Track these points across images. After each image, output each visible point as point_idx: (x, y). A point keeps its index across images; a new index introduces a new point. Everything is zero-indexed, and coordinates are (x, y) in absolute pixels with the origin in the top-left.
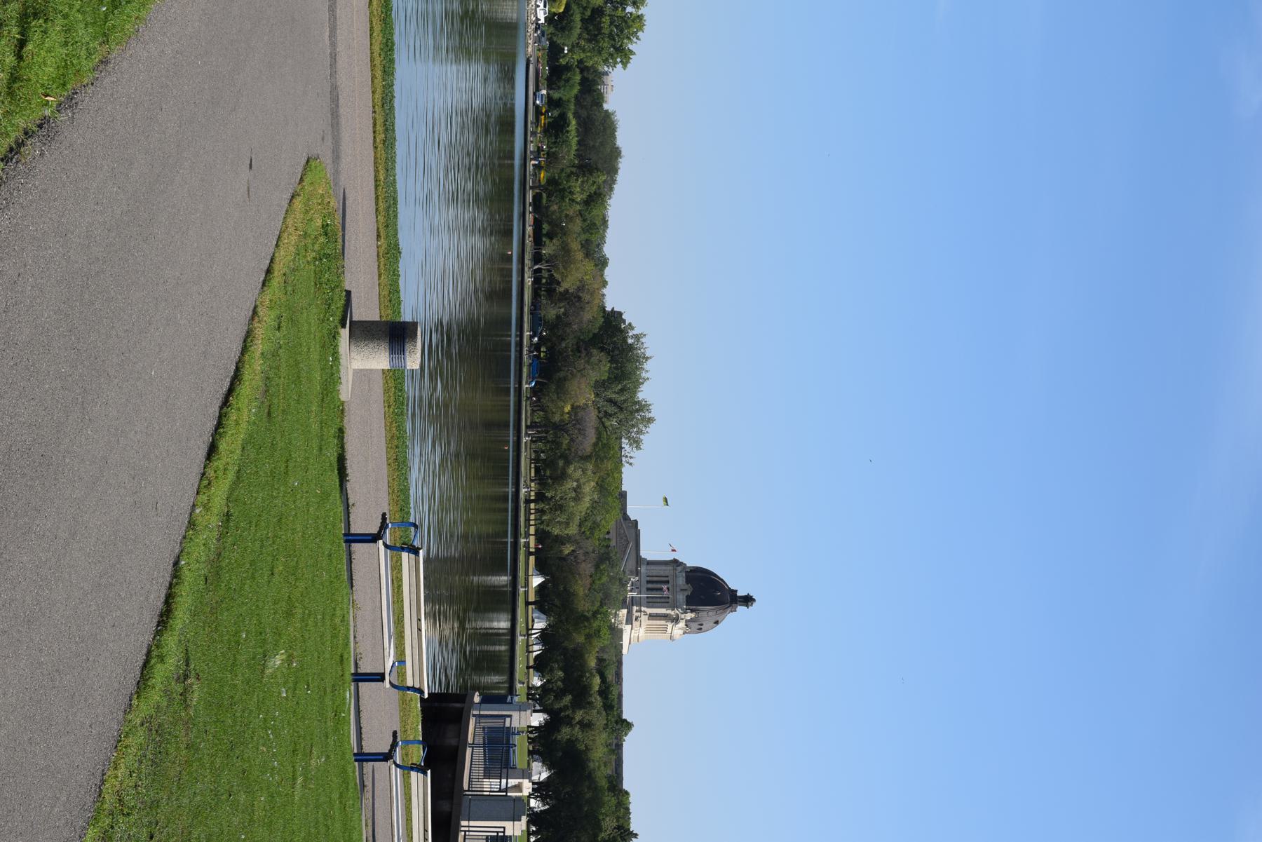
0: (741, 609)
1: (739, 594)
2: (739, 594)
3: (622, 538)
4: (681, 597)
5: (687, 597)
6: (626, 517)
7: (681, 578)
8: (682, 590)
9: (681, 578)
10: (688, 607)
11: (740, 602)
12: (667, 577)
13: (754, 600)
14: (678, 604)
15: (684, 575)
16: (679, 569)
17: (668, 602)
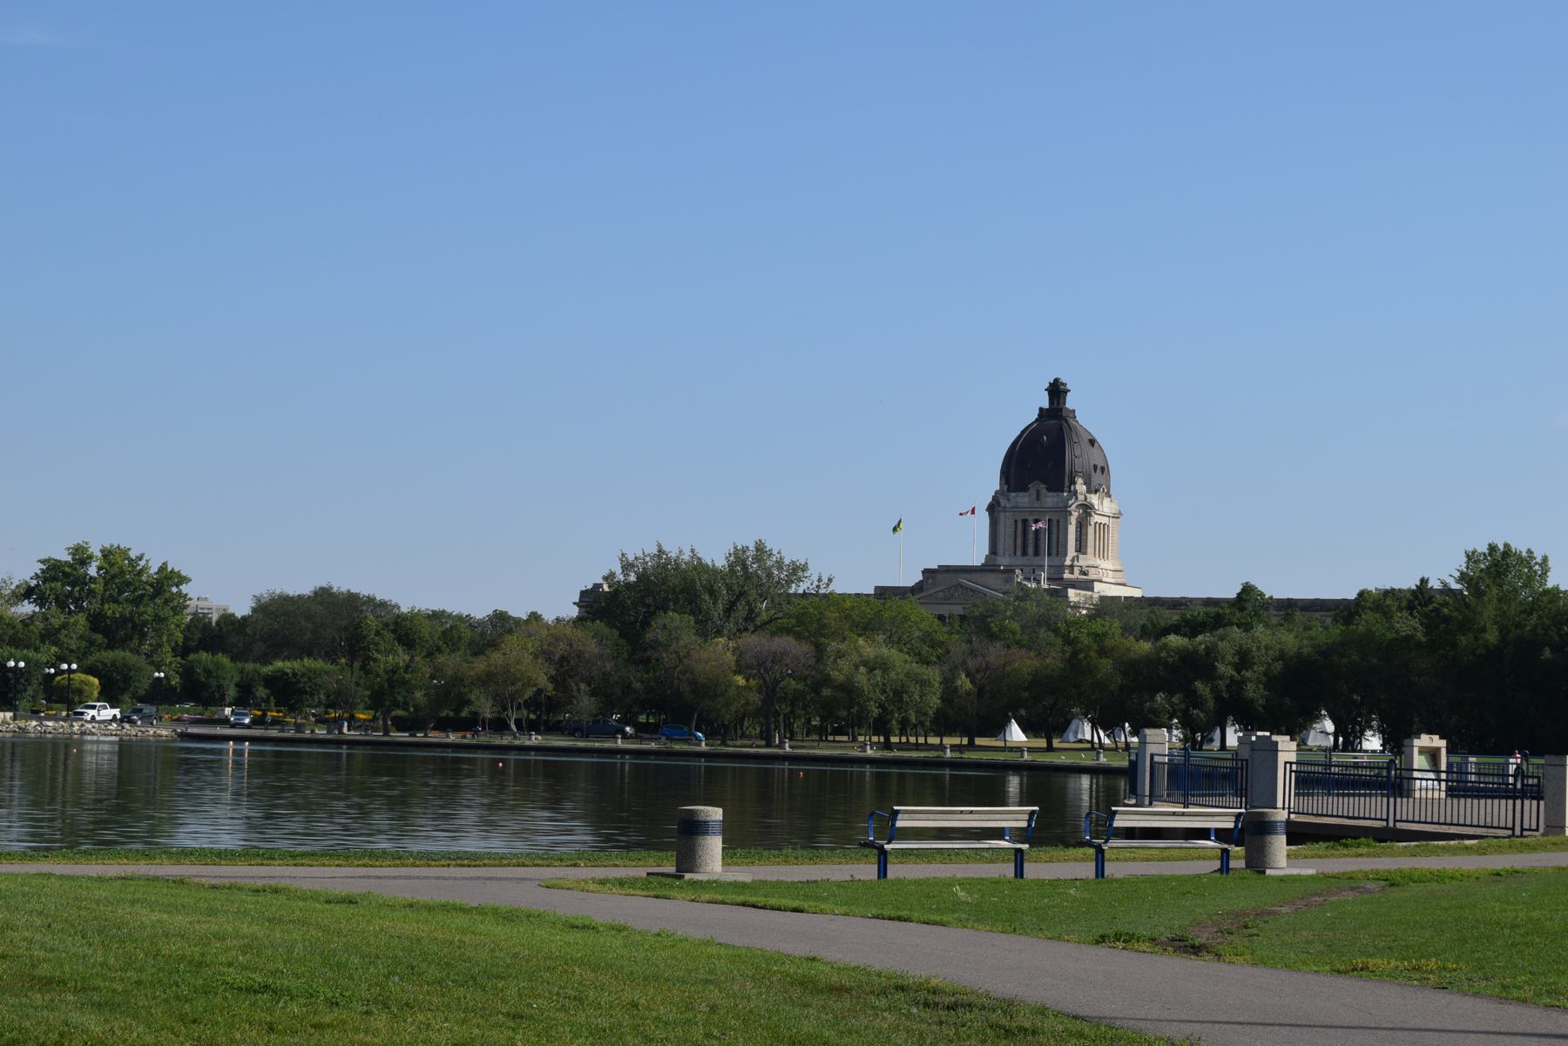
0: (1070, 402)
1: (1046, 405)
2: (1046, 405)
5: (1049, 490)
6: (917, 589)
7: (1019, 500)
8: (1038, 498)
9: (1019, 500)
10: (1066, 489)
11: (1058, 403)
12: (1016, 521)
13: (1056, 380)
14: (1061, 505)
15: (1013, 494)
16: (1003, 502)
17: (1058, 521)
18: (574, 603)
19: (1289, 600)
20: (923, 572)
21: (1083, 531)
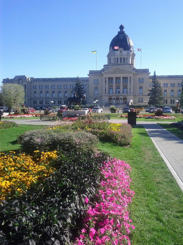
0: (124, 30)
1: (120, 31)
2: (120, 31)
5: (124, 50)
6: (103, 70)
8: (121, 52)
11: (123, 30)
13: (122, 25)
18: (2, 82)
20: (104, 66)
21: (132, 61)
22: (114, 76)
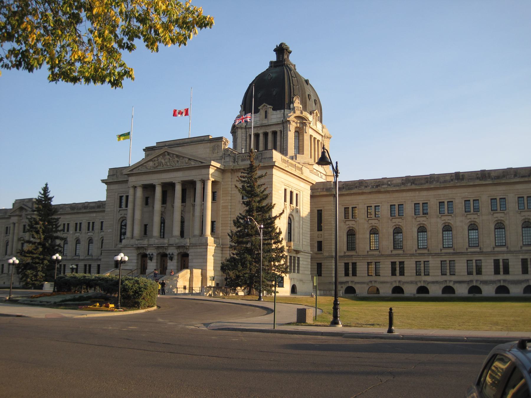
3: (160, 164)
4: (274, 116)
5: (274, 109)
13: (281, 45)
19: (483, 172)
21: (301, 138)
22: (157, 180)
